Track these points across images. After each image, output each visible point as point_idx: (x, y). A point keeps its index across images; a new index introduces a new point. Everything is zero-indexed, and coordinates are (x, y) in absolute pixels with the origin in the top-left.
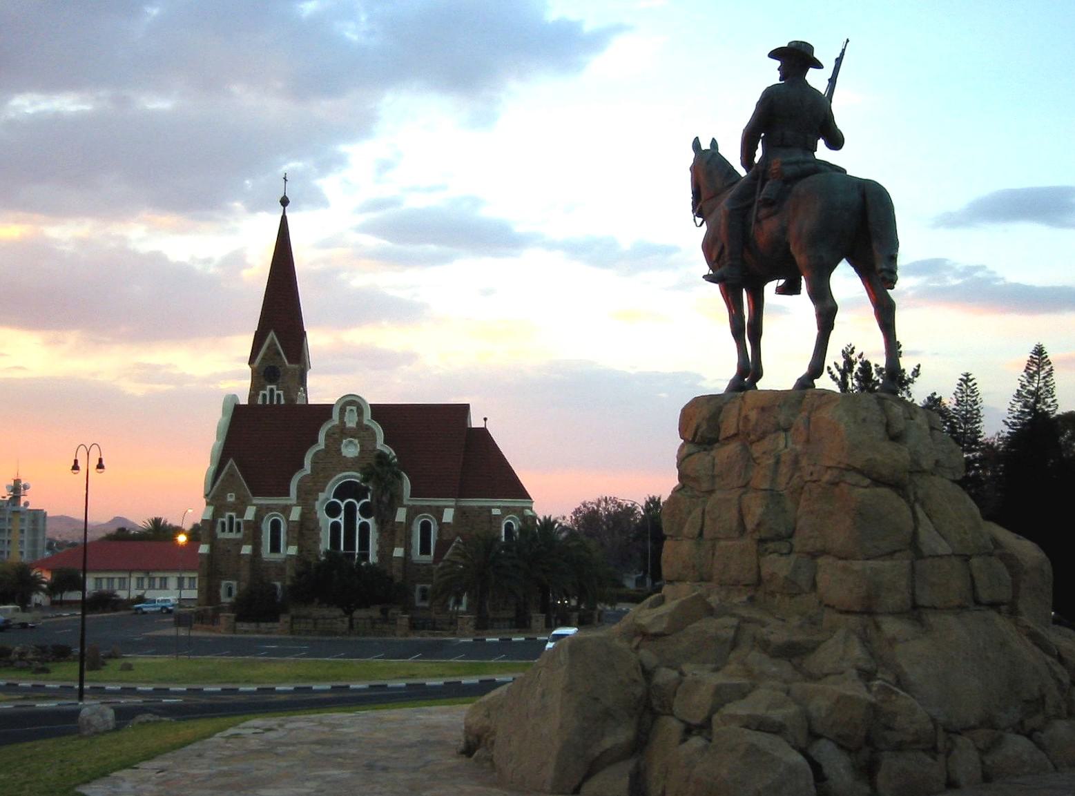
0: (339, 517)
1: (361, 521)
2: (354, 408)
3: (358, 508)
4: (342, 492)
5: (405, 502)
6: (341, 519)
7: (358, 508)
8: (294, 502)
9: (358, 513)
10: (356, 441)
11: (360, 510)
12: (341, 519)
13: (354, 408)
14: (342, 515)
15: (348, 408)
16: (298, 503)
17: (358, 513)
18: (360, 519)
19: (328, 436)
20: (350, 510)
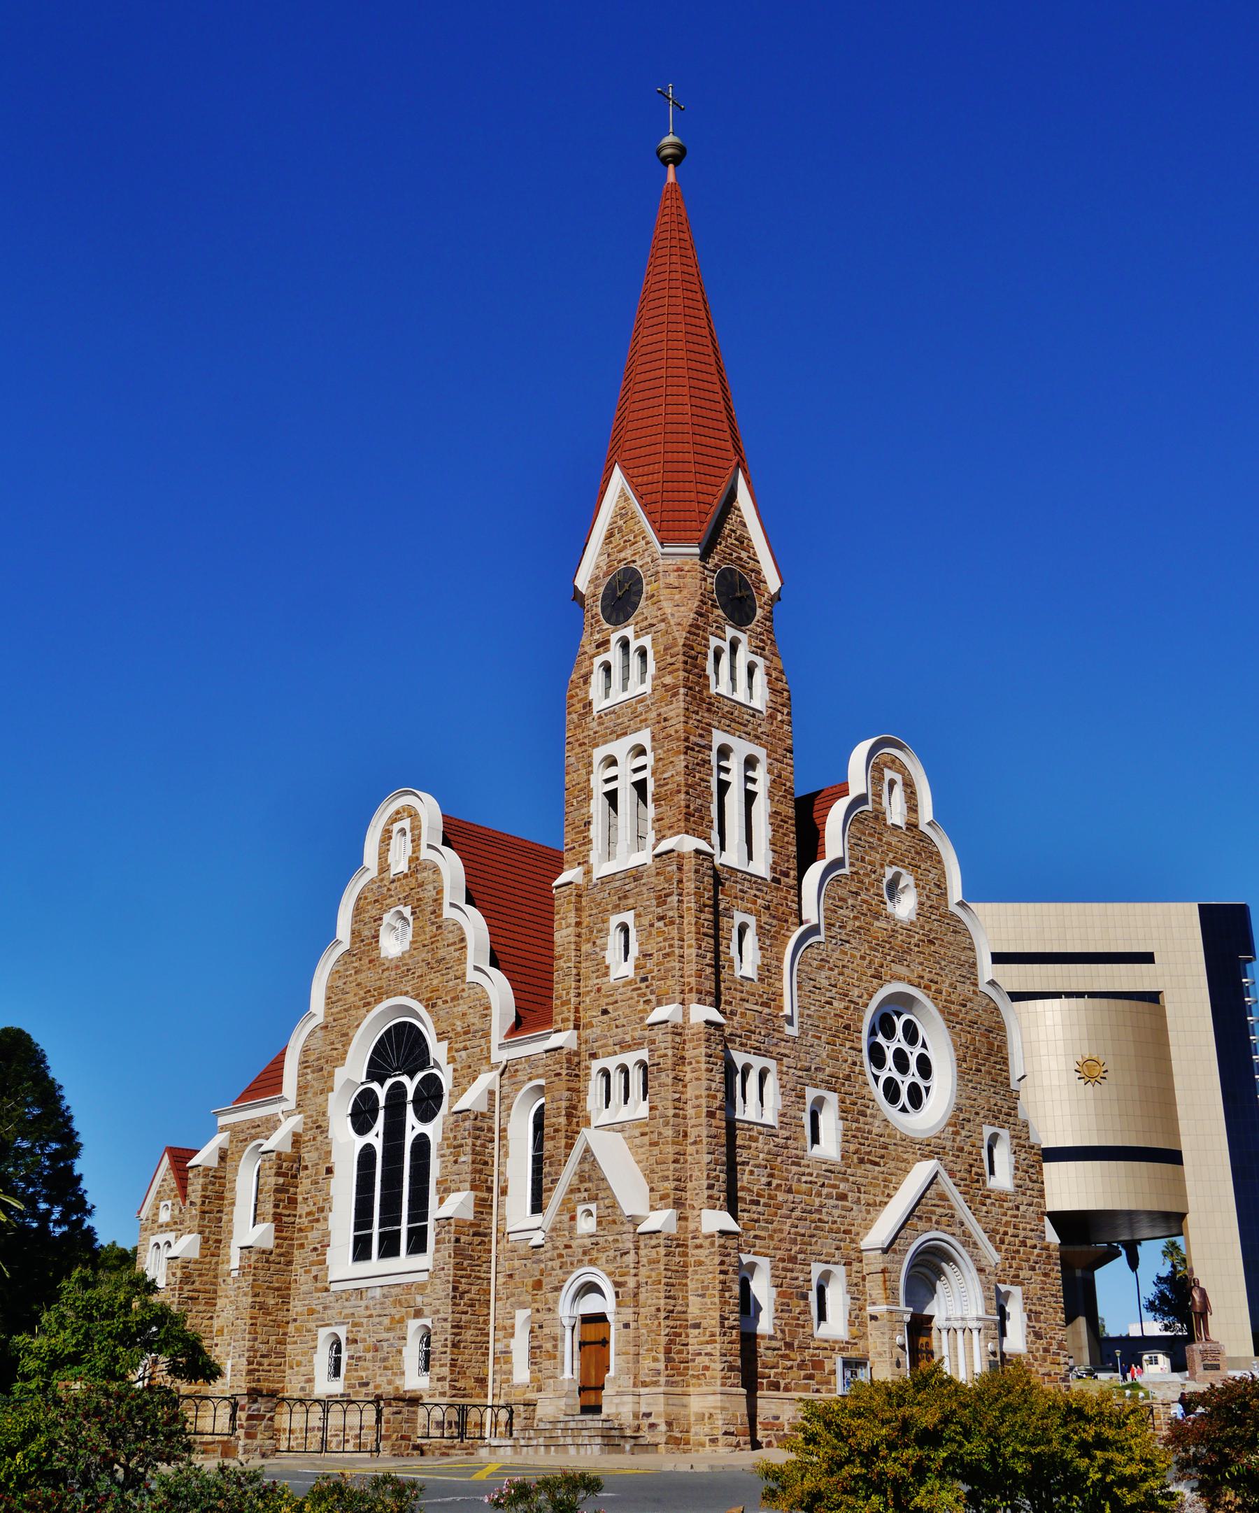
0: (374, 1131)
1: (416, 1132)
2: (406, 824)
3: (410, 1097)
6: (377, 1135)
7: (410, 1097)
8: (291, 1105)
9: (410, 1109)
10: (407, 911)
13: (406, 824)
16: (298, 1106)
17: (410, 1109)
18: (413, 1128)
19: (358, 911)
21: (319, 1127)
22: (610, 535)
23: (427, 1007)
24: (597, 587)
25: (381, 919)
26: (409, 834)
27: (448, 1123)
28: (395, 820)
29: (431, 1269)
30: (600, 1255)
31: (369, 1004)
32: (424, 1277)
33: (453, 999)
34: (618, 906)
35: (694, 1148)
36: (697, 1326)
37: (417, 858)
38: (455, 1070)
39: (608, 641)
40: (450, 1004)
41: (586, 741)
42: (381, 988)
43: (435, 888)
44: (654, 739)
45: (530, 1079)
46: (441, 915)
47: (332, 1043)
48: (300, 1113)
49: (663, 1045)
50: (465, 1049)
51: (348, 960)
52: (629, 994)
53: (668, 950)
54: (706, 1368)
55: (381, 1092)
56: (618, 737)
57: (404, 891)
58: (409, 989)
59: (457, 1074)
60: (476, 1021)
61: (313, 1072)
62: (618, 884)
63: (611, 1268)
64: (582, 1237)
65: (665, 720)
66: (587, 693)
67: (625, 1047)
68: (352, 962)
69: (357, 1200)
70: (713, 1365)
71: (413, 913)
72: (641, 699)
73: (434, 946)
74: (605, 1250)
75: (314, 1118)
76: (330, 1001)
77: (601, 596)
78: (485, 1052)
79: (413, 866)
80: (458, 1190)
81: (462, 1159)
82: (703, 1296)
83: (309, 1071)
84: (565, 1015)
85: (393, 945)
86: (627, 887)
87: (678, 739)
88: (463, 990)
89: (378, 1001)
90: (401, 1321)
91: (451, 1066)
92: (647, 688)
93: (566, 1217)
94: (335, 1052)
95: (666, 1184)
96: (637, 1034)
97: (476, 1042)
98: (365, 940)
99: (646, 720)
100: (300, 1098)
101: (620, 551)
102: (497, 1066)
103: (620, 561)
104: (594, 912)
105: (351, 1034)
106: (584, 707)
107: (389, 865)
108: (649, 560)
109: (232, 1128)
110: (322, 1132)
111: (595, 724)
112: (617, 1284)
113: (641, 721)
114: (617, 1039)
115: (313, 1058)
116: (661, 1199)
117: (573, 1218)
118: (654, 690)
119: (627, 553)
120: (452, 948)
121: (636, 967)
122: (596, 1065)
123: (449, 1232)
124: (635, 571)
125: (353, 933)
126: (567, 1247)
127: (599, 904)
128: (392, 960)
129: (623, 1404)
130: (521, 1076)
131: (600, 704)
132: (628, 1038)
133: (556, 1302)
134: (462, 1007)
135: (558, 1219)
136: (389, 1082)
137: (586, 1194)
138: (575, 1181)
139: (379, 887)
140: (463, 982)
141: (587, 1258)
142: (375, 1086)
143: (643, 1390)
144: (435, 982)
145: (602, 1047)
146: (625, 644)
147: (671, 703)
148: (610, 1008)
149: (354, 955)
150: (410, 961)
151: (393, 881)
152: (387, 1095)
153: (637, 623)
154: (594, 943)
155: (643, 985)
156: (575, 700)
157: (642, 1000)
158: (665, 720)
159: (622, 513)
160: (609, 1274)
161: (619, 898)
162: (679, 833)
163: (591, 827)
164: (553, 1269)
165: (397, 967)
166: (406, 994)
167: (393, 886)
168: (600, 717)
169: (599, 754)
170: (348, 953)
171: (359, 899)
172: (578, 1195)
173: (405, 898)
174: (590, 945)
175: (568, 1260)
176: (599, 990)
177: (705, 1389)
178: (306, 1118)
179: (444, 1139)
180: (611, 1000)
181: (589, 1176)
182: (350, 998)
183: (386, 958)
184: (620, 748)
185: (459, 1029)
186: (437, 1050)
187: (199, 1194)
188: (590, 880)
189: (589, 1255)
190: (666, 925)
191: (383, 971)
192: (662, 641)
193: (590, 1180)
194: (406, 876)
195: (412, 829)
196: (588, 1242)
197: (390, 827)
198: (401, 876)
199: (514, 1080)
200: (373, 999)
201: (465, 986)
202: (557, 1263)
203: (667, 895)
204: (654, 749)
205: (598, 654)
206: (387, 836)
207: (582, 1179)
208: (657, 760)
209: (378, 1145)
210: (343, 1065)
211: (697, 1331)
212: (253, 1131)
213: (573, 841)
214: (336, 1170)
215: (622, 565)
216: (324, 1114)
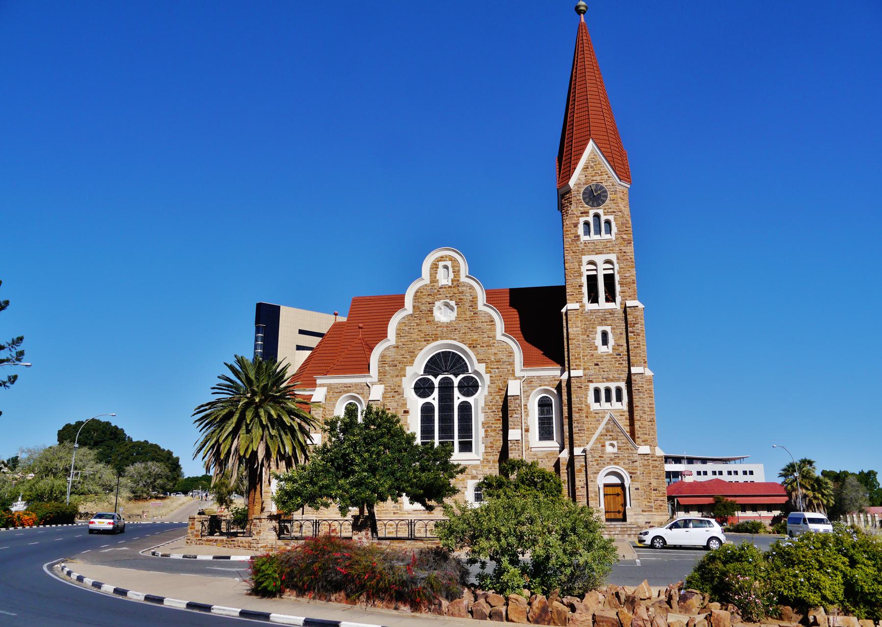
1: (460, 401)
2: (449, 264)
3: (456, 384)
4: (434, 366)
5: (518, 373)
6: (434, 399)
7: (456, 384)
9: (456, 390)
10: (453, 303)
11: (458, 387)
12: (434, 399)
14: (436, 393)
15: (441, 264)
18: (459, 398)
19: (416, 297)
20: (446, 388)
21: (396, 391)
22: (586, 168)
23: (470, 347)
24: (579, 187)
25: (434, 303)
26: (451, 269)
27: (488, 399)
28: (441, 261)
29: (482, 459)
30: (620, 461)
31: (428, 340)
32: (478, 462)
33: (487, 346)
34: (600, 323)
35: (650, 423)
36: (654, 490)
37: (458, 281)
38: (491, 377)
39: (588, 212)
40: (485, 348)
41: (577, 251)
42: (436, 334)
43: (471, 296)
44: (618, 258)
45: (541, 386)
46: (477, 308)
47: (403, 355)
48: (381, 384)
49: (640, 383)
50: (498, 368)
51: (411, 318)
52: (610, 359)
53: (636, 345)
54: (661, 506)
55: (436, 381)
56: (597, 254)
57: (449, 293)
58: (457, 337)
59: (492, 378)
60: (504, 357)
61: (390, 366)
62: (601, 314)
63: (626, 466)
64: (610, 454)
65: (625, 252)
66: (576, 231)
67: (608, 380)
68: (415, 320)
69: (421, 426)
70: (664, 504)
71: (456, 304)
72: (609, 241)
73: (473, 321)
74: (623, 459)
75: (393, 387)
76: (398, 335)
77: (582, 192)
78: (511, 371)
79: (455, 283)
80: (514, 428)
81: (516, 416)
82: (658, 479)
83: (386, 365)
84: (578, 363)
85: (443, 315)
86: (607, 316)
87: (632, 262)
88: (494, 343)
89: (436, 340)
90: (463, 480)
91: (488, 375)
92: (613, 237)
93: (599, 445)
94: (405, 360)
95: (645, 436)
96: (616, 376)
97: (505, 366)
98: (424, 312)
99: (613, 250)
100: (380, 377)
101: (593, 176)
102: (519, 378)
103: (593, 180)
104: (587, 323)
105: (416, 353)
106: (575, 237)
107: (438, 280)
108: (610, 184)
109: (330, 387)
110: (399, 394)
111: (582, 246)
112: (630, 473)
113: (610, 250)
114: (604, 376)
115: (388, 360)
116: (643, 442)
117: (603, 446)
118: (617, 239)
119: (598, 178)
120: (485, 324)
121: (613, 349)
122: (592, 386)
123: (518, 446)
124: (602, 188)
125: (414, 307)
126: (600, 457)
127: (590, 321)
128: (443, 323)
129: (638, 518)
130: (534, 384)
131: (584, 238)
132: (611, 377)
133: (595, 478)
134: (494, 350)
135: (594, 445)
136: (440, 377)
137: (611, 437)
138: (604, 432)
139: (431, 289)
140: (495, 340)
141: (612, 462)
142: (431, 377)
143: (644, 513)
144: (475, 337)
145: (596, 378)
146: (597, 216)
147: (627, 246)
148: (599, 363)
149: (415, 317)
150: (456, 325)
151: (441, 288)
152: (439, 382)
153: (605, 209)
154: (588, 336)
155: (618, 357)
156: (569, 233)
157: (617, 363)
158: (625, 252)
159: (592, 160)
160: (626, 469)
161: (602, 320)
162: (635, 299)
163: (583, 288)
164: (593, 465)
165: (447, 327)
166: (455, 339)
167: (441, 290)
168: (585, 243)
169: (586, 259)
170: (411, 315)
171: (417, 292)
172: (605, 437)
173: (450, 297)
174: (586, 336)
175: (602, 462)
176: (592, 355)
177: (660, 513)
178: (385, 386)
179: (485, 405)
180: (601, 360)
181: (612, 430)
182: (414, 336)
183: (439, 322)
184: (599, 259)
185: (493, 359)
186: (476, 366)
187: (321, 415)
188: (584, 310)
189: (614, 460)
190: (634, 335)
191: (437, 327)
192: (620, 221)
193: (612, 431)
194: (450, 287)
195: (453, 267)
196: (613, 456)
197: (437, 263)
198: (447, 286)
199: (530, 385)
200: (431, 339)
201: (496, 342)
202: (595, 463)
203: (635, 324)
204: (618, 263)
205: (582, 216)
206: (434, 267)
207: (608, 430)
208: (620, 268)
209: (436, 404)
210: (412, 366)
211: (655, 492)
212: (346, 389)
213: (572, 292)
214: (410, 412)
215: (594, 183)
216: (399, 386)
